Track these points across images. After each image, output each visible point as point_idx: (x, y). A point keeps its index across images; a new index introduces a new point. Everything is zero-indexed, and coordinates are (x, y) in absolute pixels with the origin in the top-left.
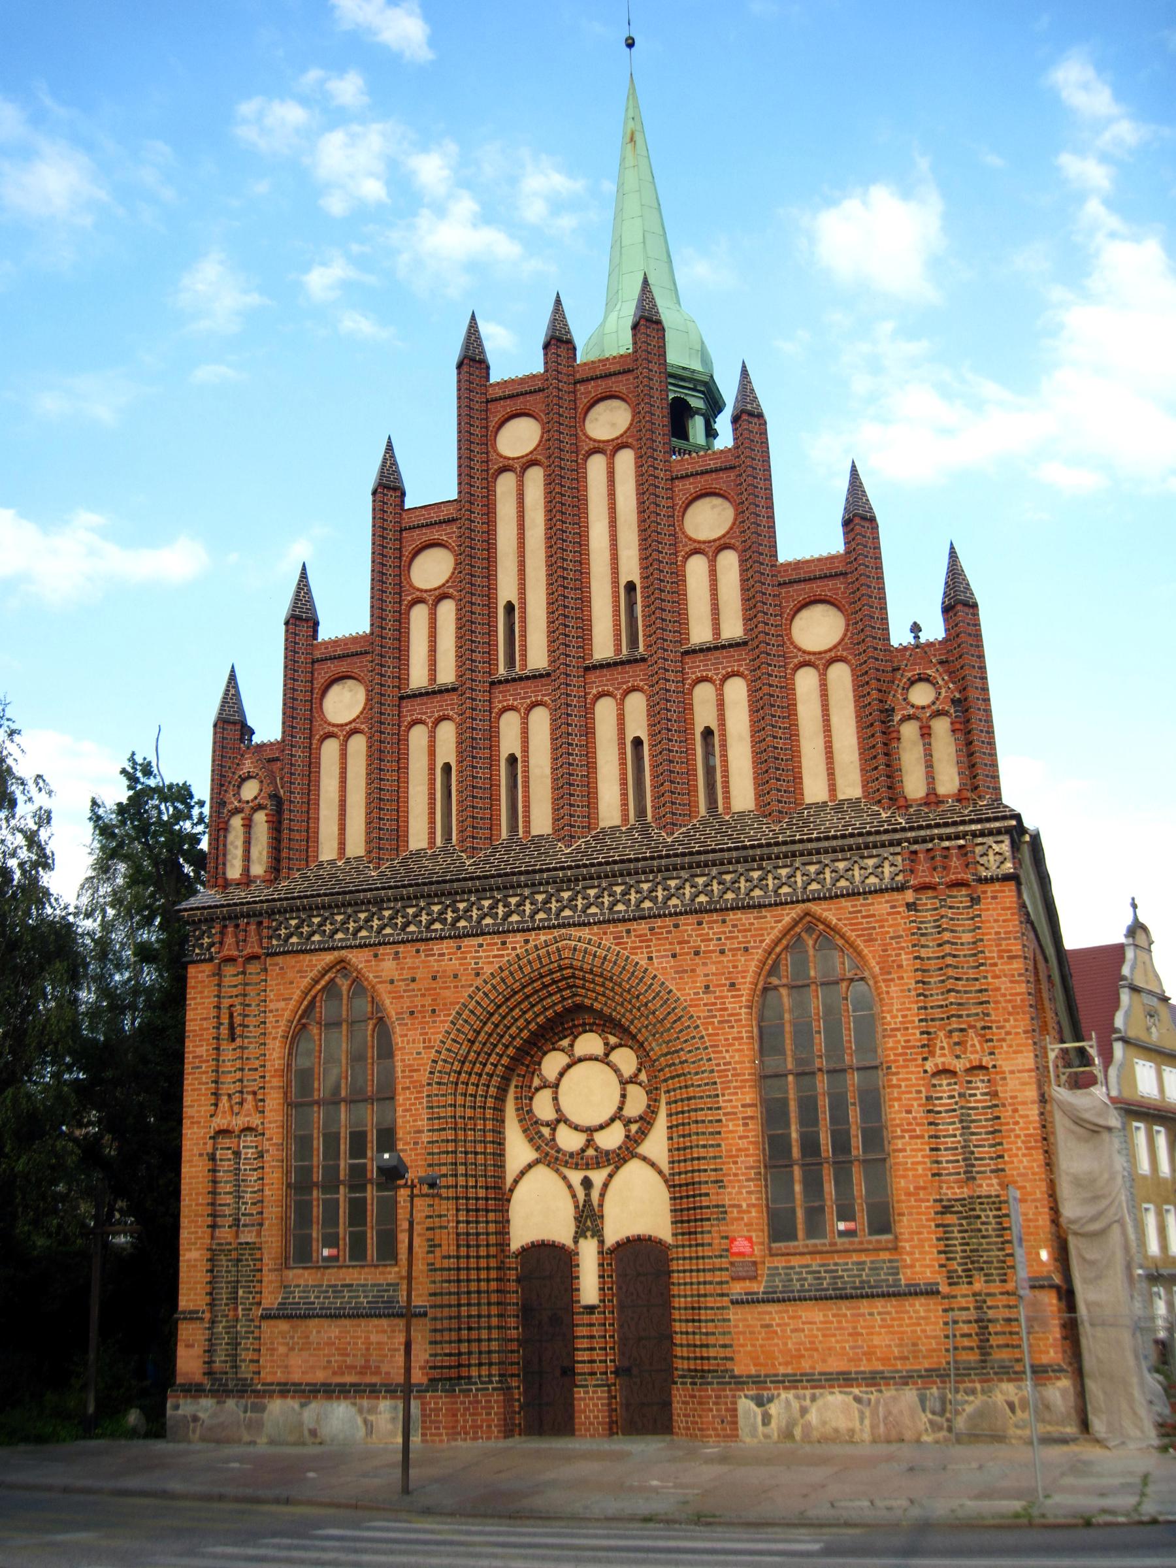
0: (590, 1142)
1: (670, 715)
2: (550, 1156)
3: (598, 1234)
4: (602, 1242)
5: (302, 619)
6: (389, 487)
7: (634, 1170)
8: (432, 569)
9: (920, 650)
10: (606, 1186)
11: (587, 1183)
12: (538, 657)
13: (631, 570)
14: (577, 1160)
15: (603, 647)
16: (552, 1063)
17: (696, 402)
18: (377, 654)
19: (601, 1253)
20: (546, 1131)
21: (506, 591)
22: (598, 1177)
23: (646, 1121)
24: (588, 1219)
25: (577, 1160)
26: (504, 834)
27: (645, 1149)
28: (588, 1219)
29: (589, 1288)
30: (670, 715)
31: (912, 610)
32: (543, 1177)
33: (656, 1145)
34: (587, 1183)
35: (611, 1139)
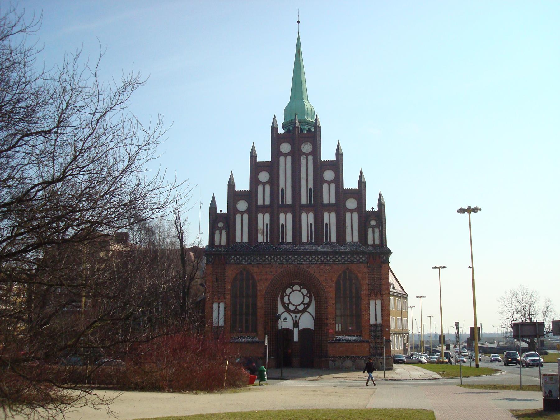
1: (318, 219)
2: (288, 310)
3: (298, 327)
5: (231, 185)
6: (253, 156)
7: (306, 314)
8: (264, 176)
9: (373, 212)
11: (296, 317)
12: (289, 201)
13: (311, 185)
14: (293, 312)
15: (304, 201)
16: (288, 291)
18: (249, 196)
20: (287, 305)
21: (282, 185)
22: (298, 315)
23: (309, 304)
24: (296, 324)
25: (293, 312)
26: (280, 241)
27: (308, 310)
28: (296, 324)
29: (296, 338)
30: (318, 219)
31: (371, 205)
32: (286, 315)
33: (312, 309)
34: (296, 317)
35: (301, 308)
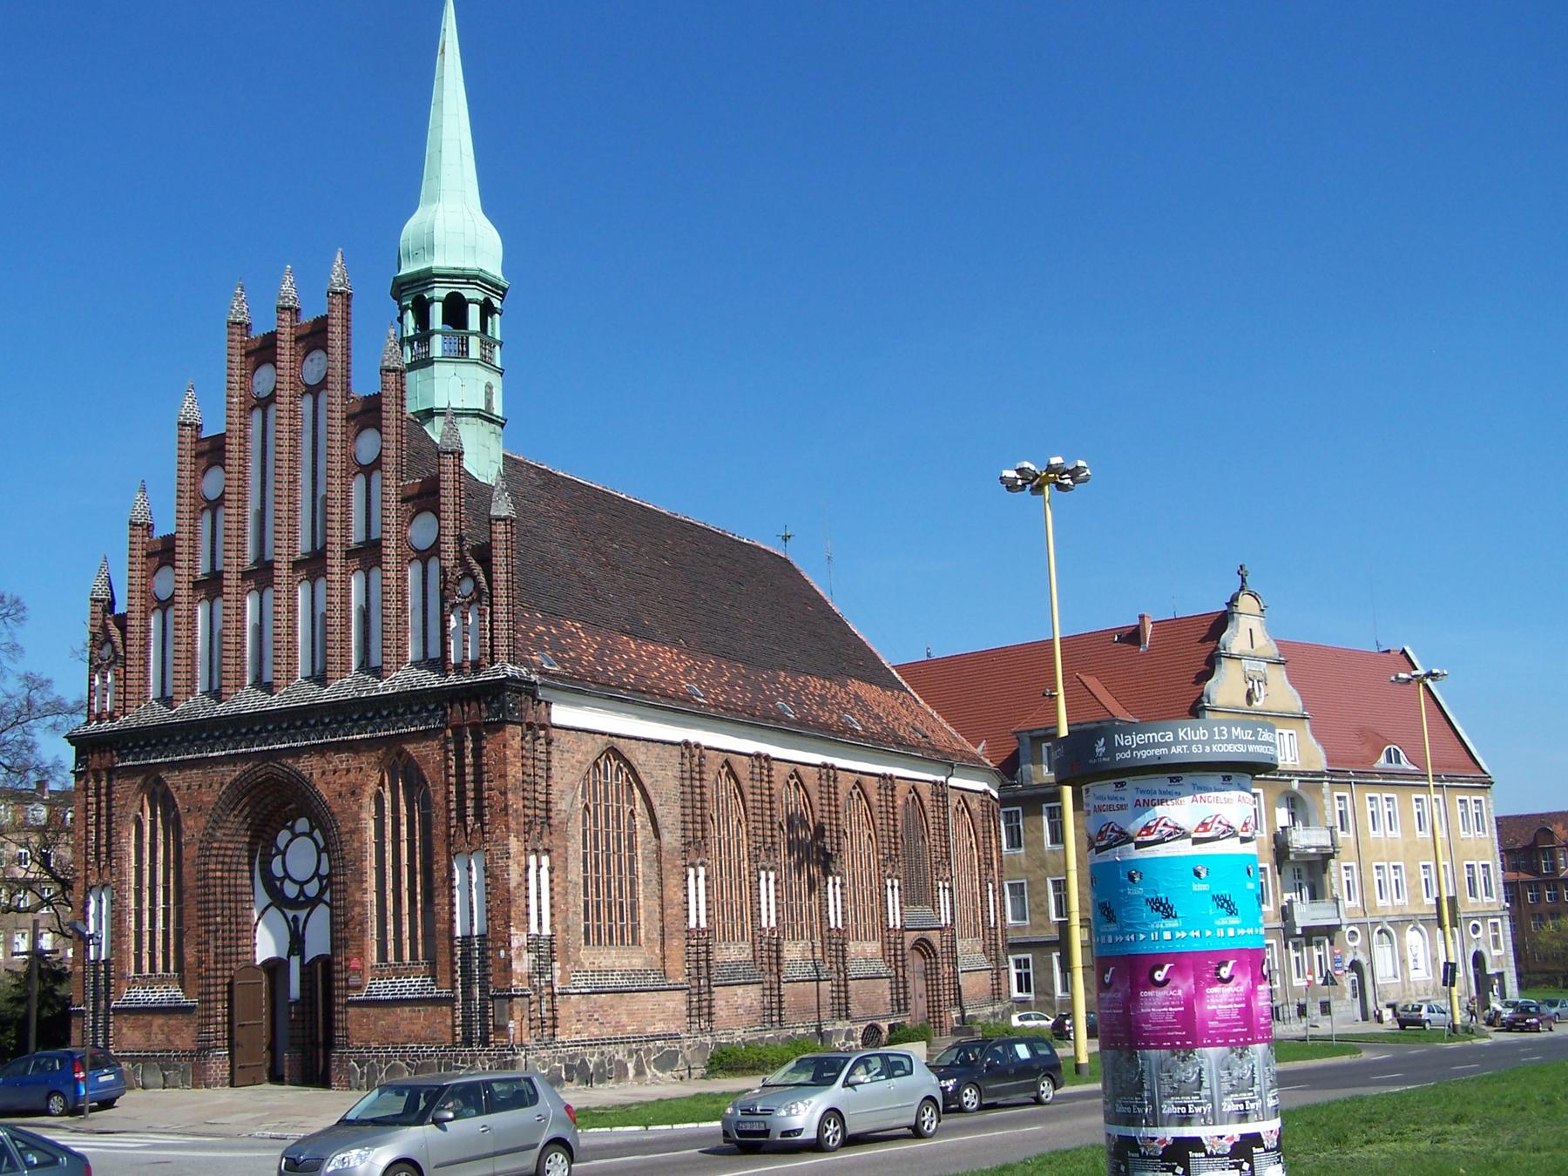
0: (302, 892)
2: (279, 899)
4: (302, 958)
10: (306, 921)
11: (295, 918)
14: (294, 904)
16: (283, 837)
17: (469, 293)
19: (302, 965)
22: (302, 914)
24: (297, 942)
35: (312, 889)
